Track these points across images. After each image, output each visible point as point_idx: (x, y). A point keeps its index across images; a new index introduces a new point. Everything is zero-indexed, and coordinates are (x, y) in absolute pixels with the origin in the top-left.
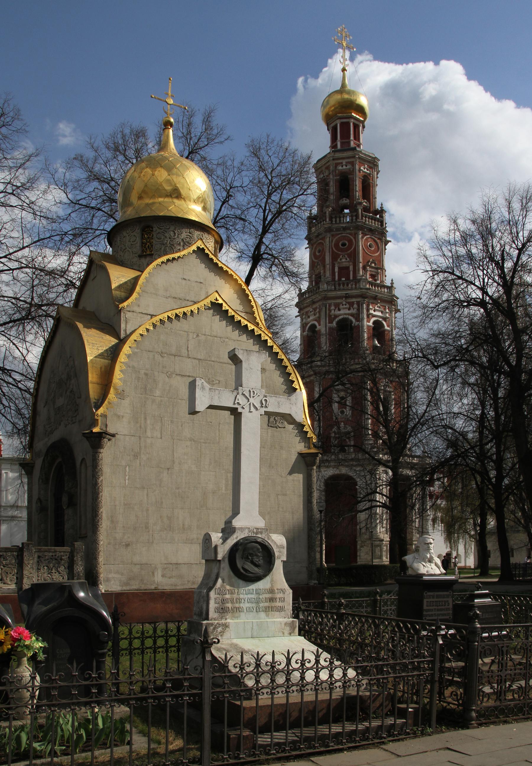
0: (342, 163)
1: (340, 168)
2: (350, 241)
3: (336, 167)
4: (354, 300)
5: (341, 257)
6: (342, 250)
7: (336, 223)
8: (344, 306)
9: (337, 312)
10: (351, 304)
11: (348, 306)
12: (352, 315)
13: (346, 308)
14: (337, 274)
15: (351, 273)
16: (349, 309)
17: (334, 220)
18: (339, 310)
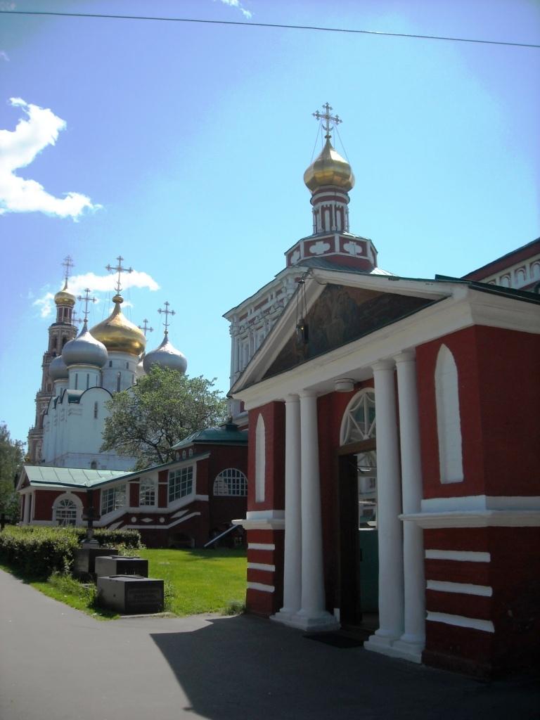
1: (54, 333)
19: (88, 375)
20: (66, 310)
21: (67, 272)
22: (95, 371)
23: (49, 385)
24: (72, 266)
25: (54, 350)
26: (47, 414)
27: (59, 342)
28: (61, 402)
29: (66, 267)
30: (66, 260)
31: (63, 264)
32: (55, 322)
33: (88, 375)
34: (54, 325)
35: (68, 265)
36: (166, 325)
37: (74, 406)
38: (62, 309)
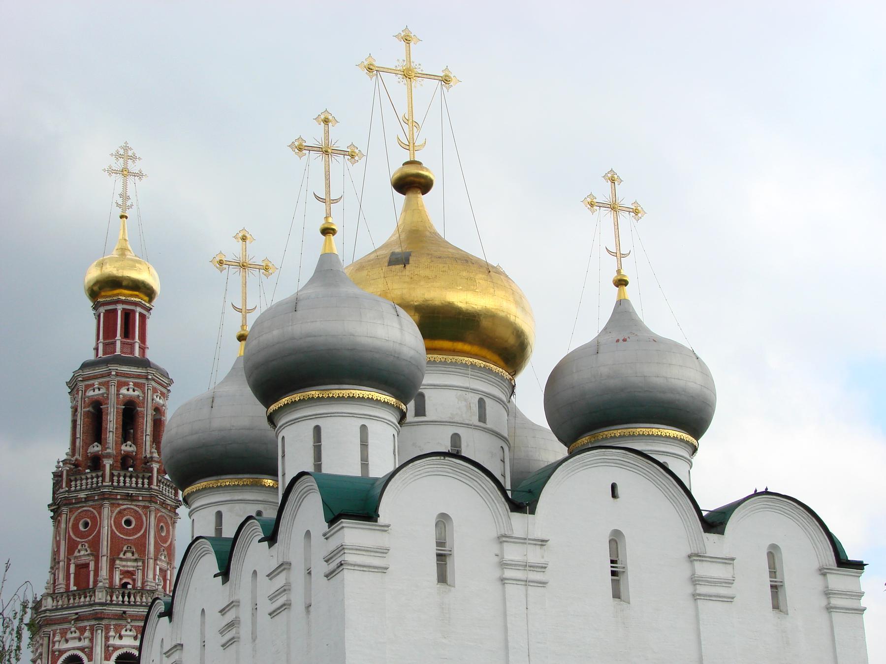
0: (93, 385)
1: (90, 393)
2: (94, 519)
3: (85, 392)
4: (86, 623)
5: (80, 547)
6: (81, 535)
7: (76, 491)
8: (74, 635)
9: (64, 646)
10: (82, 630)
11: (77, 634)
12: (82, 649)
13: (74, 638)
14: (72, 576)
15: (92, 574)
16: (80, 639)
17: (73, 483)
18: (67, 641)
19: (364, 428)
20: (128, 316)
21: (125, 196)
22: (389, 423)
23: (82, 568)
24: (140, 175)
25: (96, 448)
26: (169, 613)
27: (112, 421)
28: (271, 538)
29: (120, 178)
30: (118, 156)
31: (111, 171)
32: (91, 356)
33: (364, 428)
34: (85, 366)
35: (125, 172)
36: (619, 255)
37: (352, 533)
38: (115, 311)
